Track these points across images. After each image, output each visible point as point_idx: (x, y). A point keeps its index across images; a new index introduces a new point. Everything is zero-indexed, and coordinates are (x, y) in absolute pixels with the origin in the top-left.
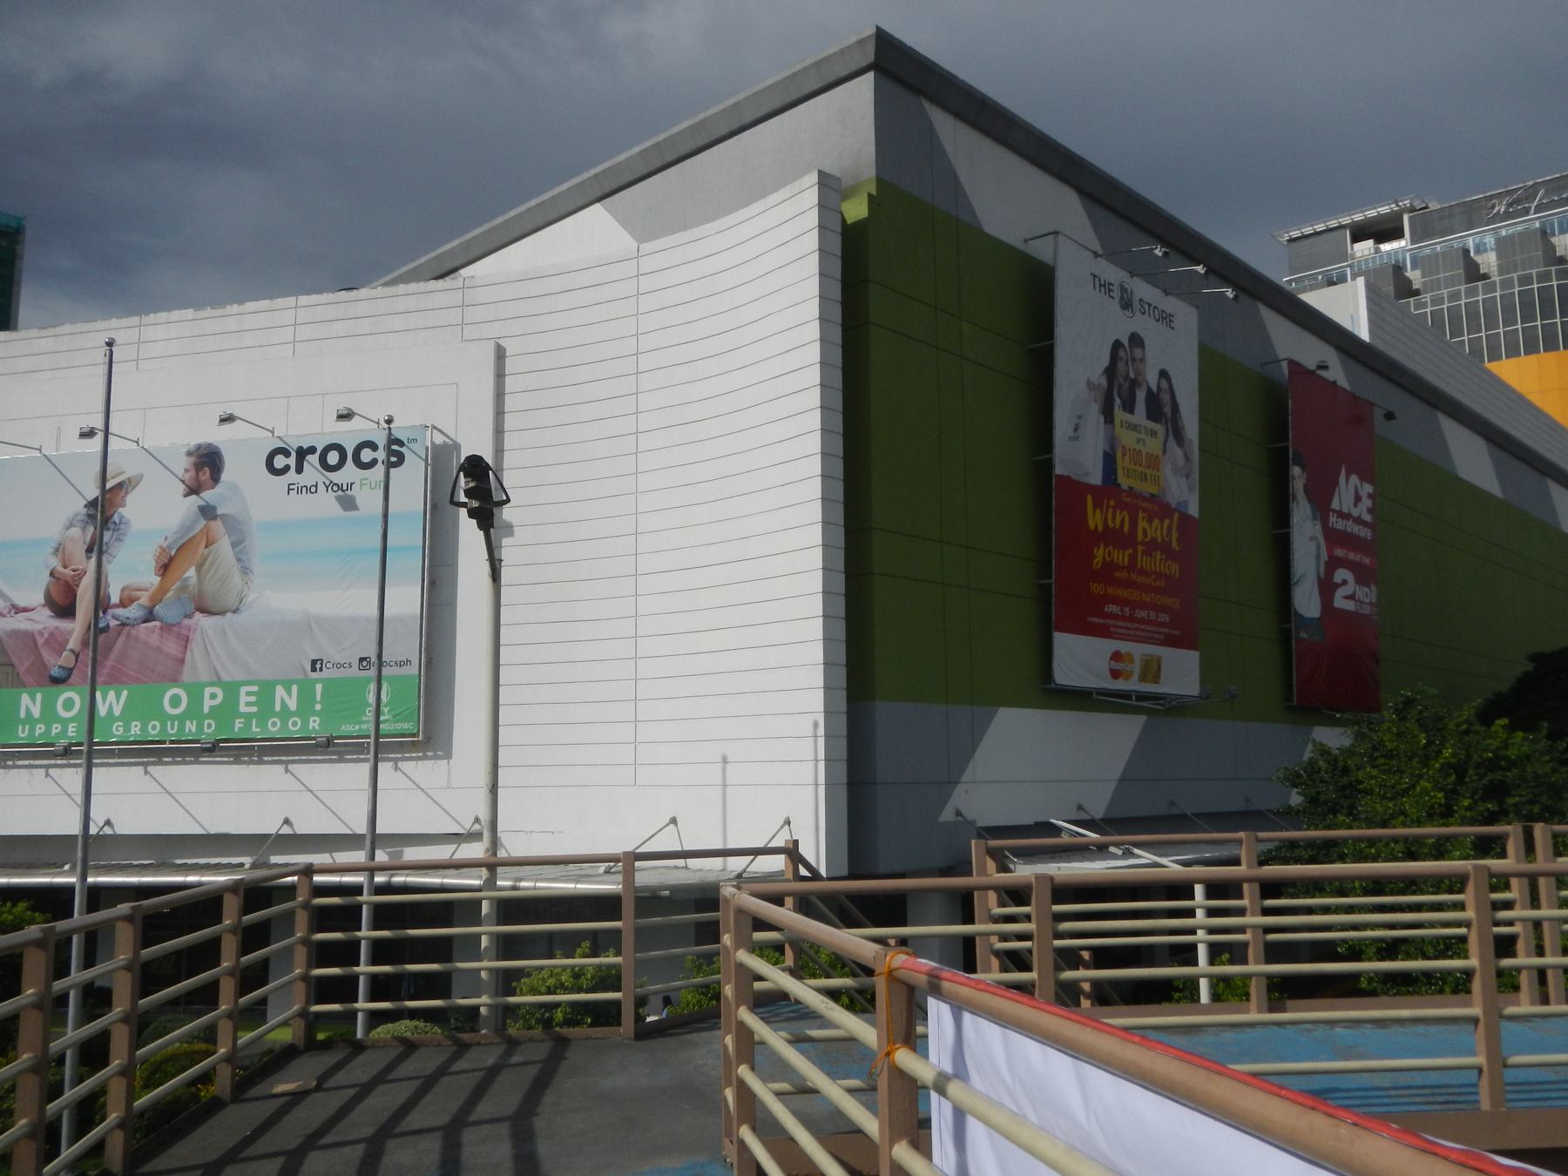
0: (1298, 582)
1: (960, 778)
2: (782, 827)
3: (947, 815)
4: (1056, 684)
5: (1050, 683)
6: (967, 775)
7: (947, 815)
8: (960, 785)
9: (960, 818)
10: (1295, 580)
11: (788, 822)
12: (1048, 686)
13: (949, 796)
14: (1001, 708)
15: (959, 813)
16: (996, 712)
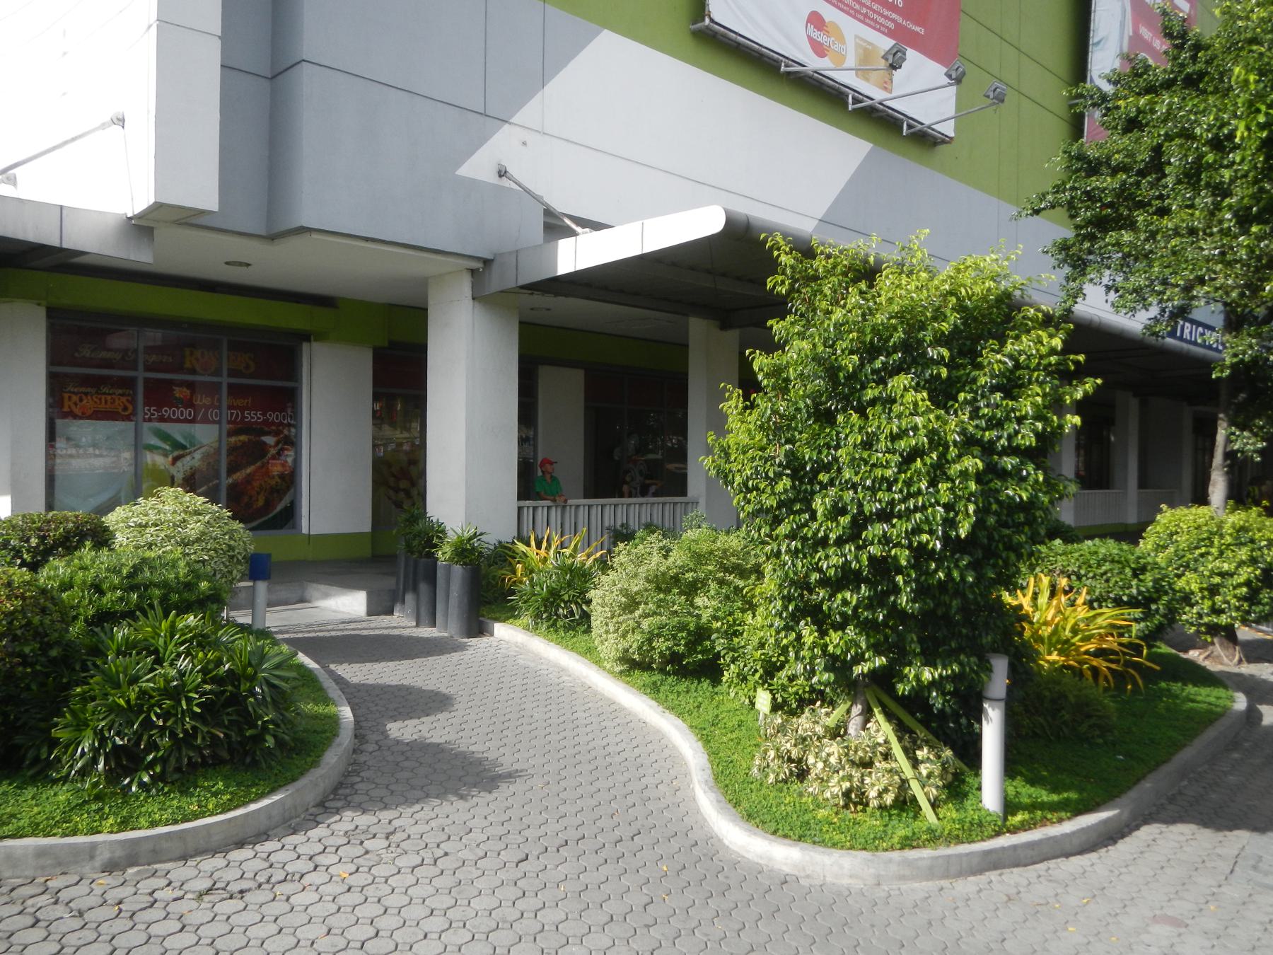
0: (1098, 43)
1: (512, 116)
2: (103, 126)
3: (478, 167)
4: (712, 21)
5: (703, 20)
6: (528, 114)
7: (478, 167)
8: (506, 126)
9: (505, 182)
10: (1096, 40)
11: (121, 121)
12: (699, 25)
13: (483, 139)
14: (606, 33)
15: (502, 173)
16: (598, 33)
